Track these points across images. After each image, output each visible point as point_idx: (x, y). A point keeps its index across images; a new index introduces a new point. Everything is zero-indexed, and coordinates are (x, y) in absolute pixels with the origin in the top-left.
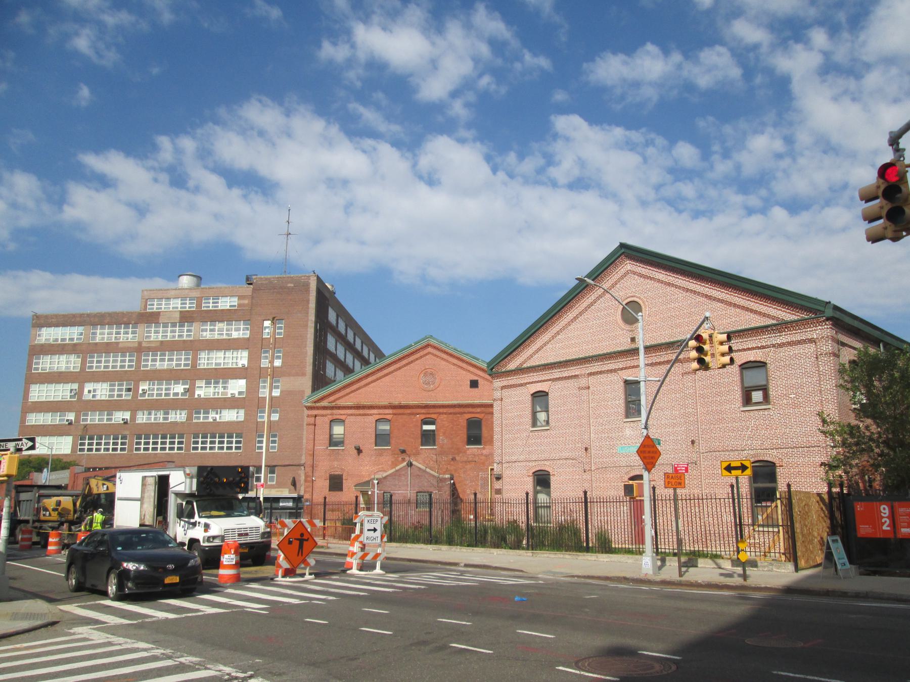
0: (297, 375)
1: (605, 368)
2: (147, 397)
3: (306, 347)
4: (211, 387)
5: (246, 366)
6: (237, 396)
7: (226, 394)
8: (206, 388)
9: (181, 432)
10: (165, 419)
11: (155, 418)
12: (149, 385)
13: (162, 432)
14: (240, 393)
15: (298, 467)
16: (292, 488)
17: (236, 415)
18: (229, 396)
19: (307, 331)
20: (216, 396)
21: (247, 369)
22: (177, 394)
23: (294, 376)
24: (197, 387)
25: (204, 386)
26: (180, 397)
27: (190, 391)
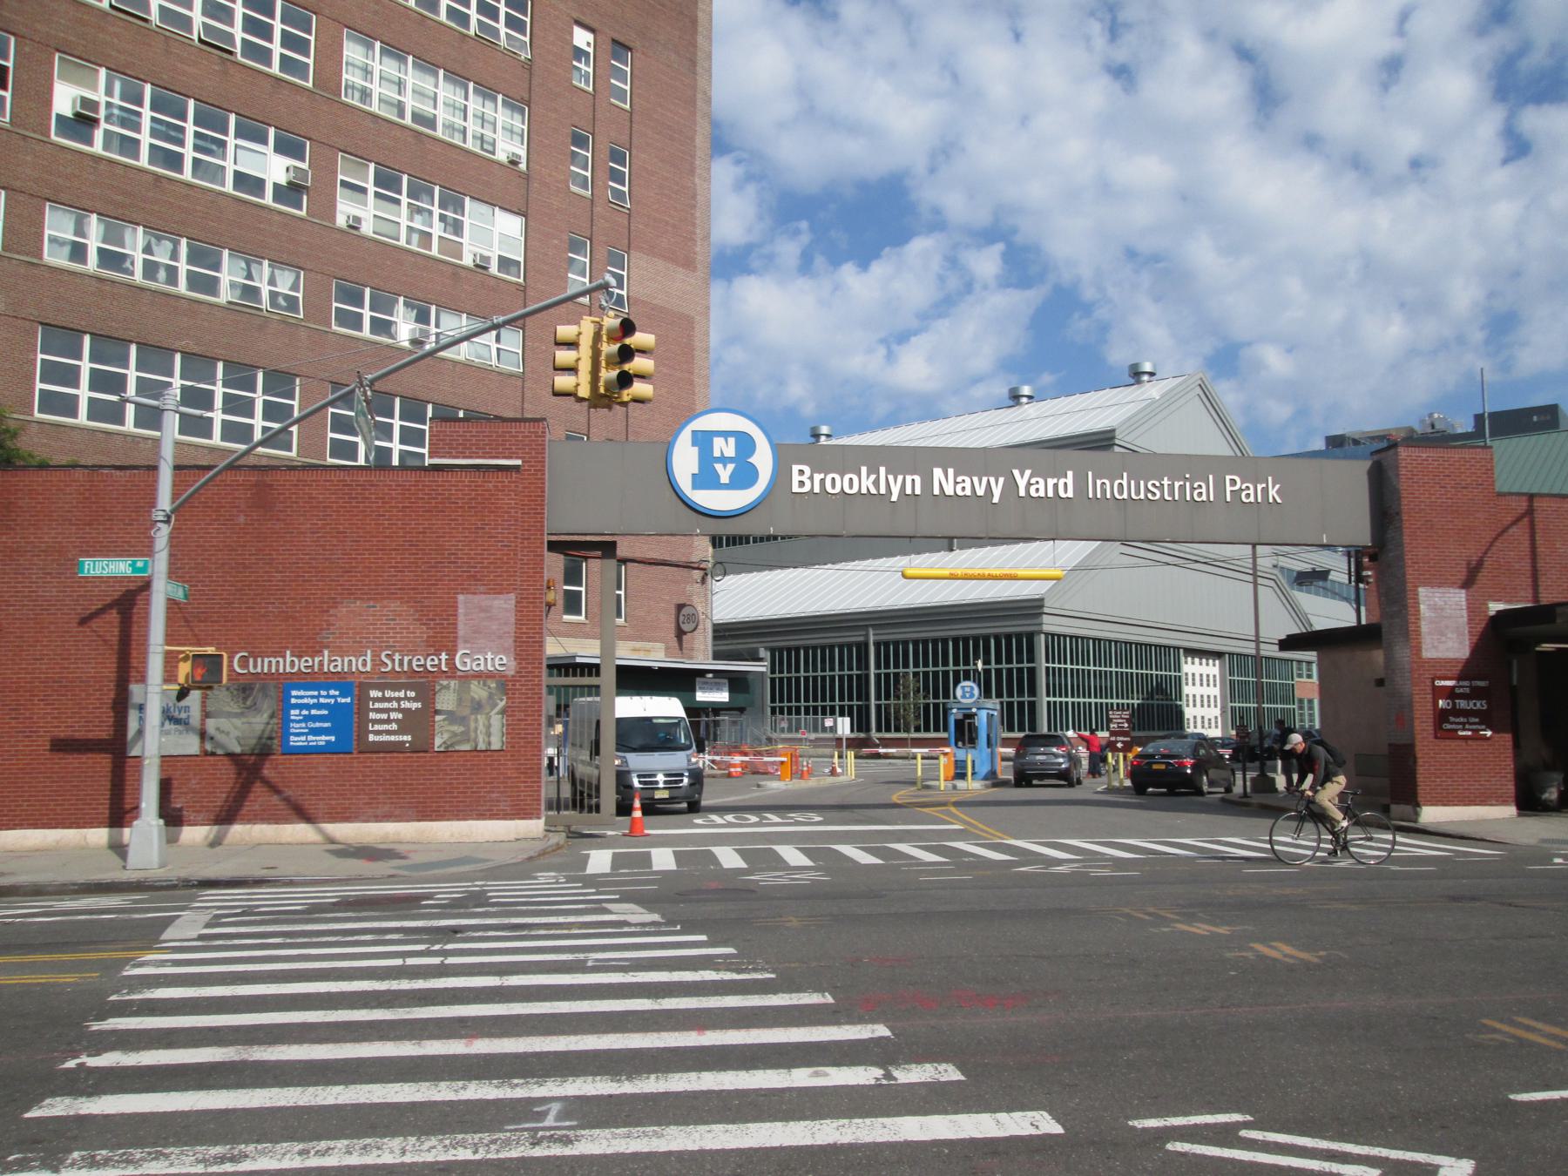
3: (692, 171)
4: (398, 202)
6: (494, 269)
7: (457, 250)
9: (283, 366)
11: (110, 259)
12: (109, 92)
14: (505, 263)
16: (674, 642)
17: (494, 346)
19: (695, 123)
20: (414, 247)
21: (526, 177)
22: (256, 185)
24: (345, 184)
25: (371, 189)
26: (268, 200)
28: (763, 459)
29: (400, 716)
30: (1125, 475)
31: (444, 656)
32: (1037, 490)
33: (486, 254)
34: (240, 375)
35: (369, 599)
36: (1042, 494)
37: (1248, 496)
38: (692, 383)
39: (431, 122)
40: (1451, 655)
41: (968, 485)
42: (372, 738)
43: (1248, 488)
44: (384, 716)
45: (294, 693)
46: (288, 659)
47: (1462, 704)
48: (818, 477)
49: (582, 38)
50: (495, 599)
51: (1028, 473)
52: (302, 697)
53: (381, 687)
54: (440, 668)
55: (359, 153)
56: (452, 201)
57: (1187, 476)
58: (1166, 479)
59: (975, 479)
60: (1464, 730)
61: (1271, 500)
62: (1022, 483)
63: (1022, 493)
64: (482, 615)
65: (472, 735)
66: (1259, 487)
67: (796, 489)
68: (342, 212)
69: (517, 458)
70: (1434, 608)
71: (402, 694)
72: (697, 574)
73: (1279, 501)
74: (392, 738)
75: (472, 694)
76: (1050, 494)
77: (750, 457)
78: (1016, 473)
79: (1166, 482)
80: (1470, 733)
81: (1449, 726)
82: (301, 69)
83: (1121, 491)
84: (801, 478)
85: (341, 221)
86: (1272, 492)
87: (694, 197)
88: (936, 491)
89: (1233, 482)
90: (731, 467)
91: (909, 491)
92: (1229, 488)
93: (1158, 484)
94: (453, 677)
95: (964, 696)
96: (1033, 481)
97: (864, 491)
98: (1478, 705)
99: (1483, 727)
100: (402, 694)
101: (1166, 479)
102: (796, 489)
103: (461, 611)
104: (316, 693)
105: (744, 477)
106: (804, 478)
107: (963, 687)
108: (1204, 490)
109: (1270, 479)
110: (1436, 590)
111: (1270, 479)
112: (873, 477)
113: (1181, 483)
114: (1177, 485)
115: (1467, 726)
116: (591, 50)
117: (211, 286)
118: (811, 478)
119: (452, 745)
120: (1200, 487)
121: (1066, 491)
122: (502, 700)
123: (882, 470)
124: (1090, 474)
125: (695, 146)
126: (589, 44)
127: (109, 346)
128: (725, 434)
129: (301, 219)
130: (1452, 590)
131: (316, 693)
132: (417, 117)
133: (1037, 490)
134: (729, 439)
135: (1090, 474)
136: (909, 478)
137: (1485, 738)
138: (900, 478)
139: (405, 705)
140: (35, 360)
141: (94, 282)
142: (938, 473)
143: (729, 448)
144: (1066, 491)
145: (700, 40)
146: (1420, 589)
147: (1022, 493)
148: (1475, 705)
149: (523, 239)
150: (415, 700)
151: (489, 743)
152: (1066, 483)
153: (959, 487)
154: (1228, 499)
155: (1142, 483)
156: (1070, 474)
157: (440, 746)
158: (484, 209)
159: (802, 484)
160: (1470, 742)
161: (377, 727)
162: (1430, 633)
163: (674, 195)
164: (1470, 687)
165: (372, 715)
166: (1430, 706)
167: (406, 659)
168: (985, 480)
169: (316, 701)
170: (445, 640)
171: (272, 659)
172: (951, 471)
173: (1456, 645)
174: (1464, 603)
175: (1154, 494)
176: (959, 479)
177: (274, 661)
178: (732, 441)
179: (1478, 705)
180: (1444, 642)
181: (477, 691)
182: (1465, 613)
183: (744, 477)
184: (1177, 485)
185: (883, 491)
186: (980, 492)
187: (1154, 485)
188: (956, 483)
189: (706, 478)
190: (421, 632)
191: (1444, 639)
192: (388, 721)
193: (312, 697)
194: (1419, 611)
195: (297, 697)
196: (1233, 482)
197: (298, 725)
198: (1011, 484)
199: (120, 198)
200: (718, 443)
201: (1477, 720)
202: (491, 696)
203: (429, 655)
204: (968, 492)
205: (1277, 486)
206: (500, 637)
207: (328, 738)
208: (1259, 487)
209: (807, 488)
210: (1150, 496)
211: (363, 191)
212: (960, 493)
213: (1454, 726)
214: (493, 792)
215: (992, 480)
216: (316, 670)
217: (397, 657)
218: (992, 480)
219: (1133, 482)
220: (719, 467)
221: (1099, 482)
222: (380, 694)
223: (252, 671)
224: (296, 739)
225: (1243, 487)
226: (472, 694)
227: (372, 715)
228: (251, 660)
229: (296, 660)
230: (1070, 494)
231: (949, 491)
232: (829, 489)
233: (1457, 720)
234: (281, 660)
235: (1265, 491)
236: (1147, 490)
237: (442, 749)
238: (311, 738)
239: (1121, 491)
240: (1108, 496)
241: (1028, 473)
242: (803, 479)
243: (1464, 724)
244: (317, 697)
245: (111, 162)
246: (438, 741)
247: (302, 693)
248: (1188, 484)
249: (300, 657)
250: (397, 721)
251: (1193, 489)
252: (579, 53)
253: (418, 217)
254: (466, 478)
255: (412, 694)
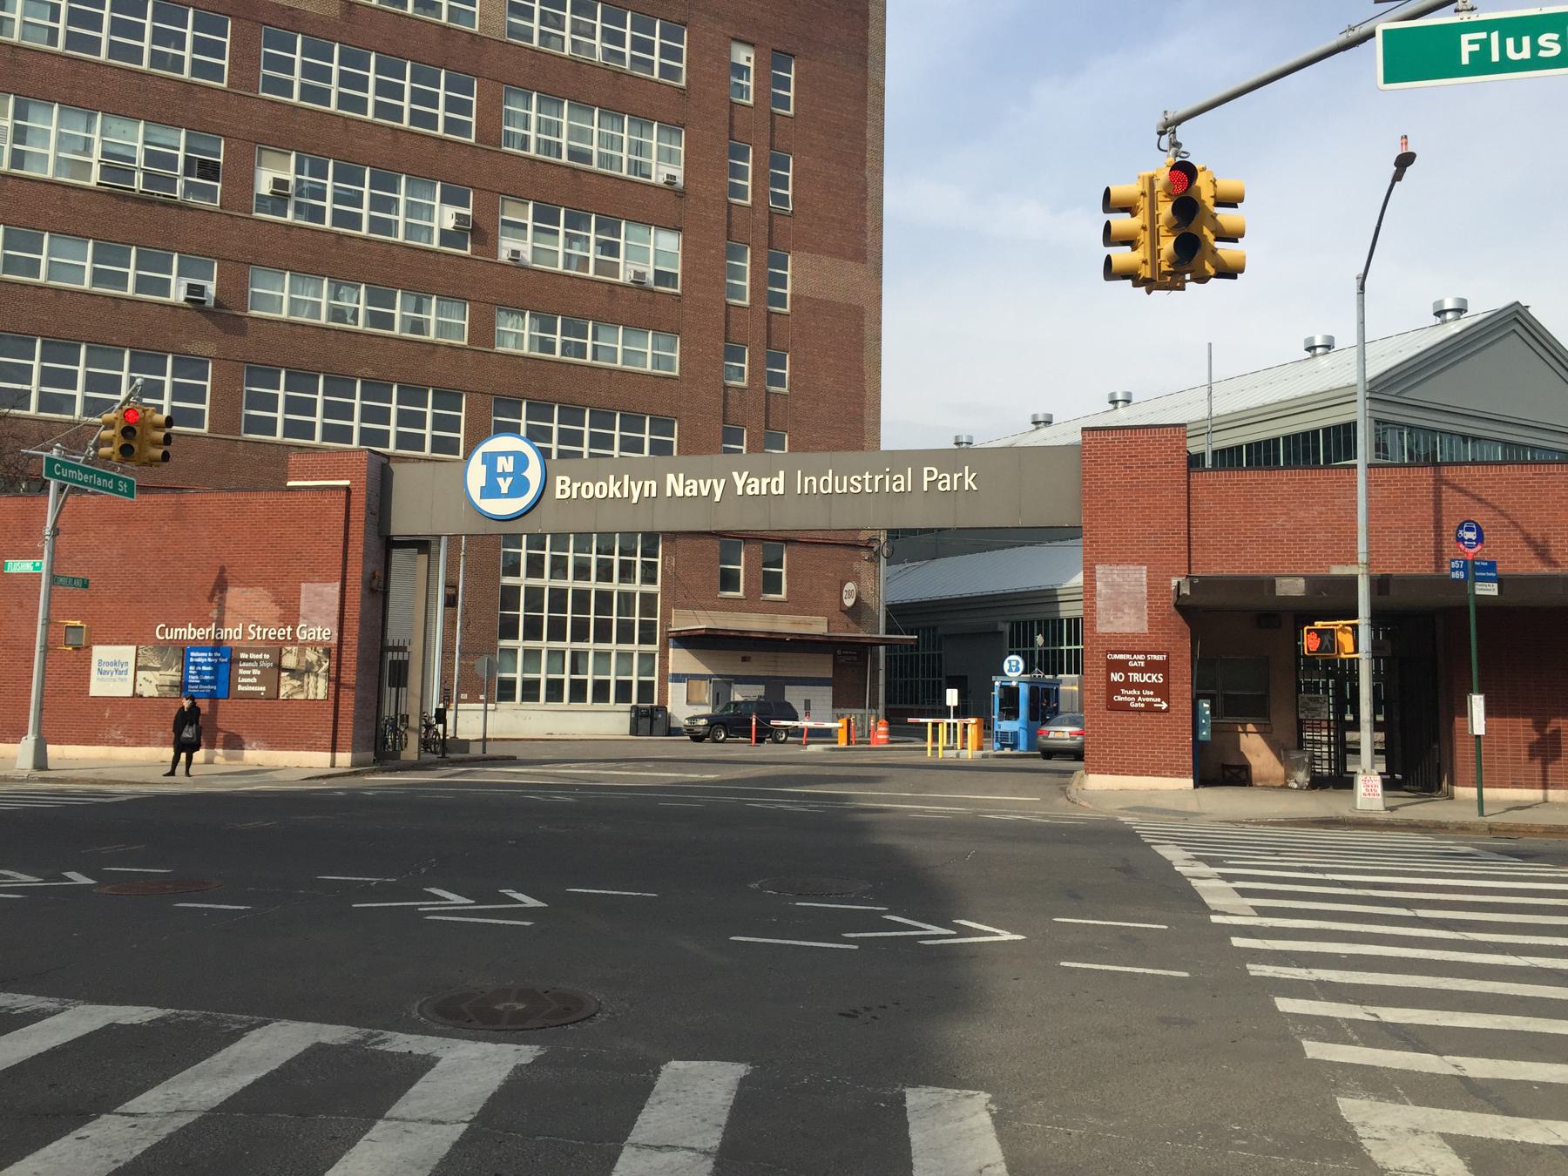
0: (837, 252)
1: (1422, 377)
2: (290, 217)
5: (680, 181)
7: (613, 269)
8: (542, 236)
10: (377, 319)
13: (371, 373)
14: (661, 277)
15: (850, 551)
18: (624, 277)
21: (681, 194)
23: (831, 254)
25: (530, 222)
27: (478, 232)
28: (534, 473)
29: (259, 672)
30: (830, 471)
31: (289, 629)
32: (753, 489)
33: (640, 269)
34: (412, 394)
35: (244, 587)
36: (756, 492)
37: (944, 485)
38: (861, 371)
39: (586, 157)
40: (1127, 630)
41: (695, 487)
42: (240, 688)
43: (944, 478)
44: (248, 672)
45: (193, 654)
46: (190, 630)
47: (1136, 677)
48: (575, 486)
49: (743, 55)
50: (326, 586)
51: (745, 474)
52: (197, 657)
53: (248, 651)
54: (286, 638)
55: (518, 195)
56: (608, 225)
57: (888, 470)
58: (867, 473)
59: (701, 482)
60: (1136, 702)
61: (967, 488)
62: (740, 484)
63: (740, 492)
64: (317, 598)
65: (306, 687)
66: (956, 476)
67: (558, 496)
68: (506, 248)
69: (347, 479)
70: (1107, 584)
71: (260, 656)
72: (865, 554)
73: (975, 488)
74: (253, 688)
75: (307, 657)
76: (764, 492)
77: (524, 471)
78: (735, 475)
79: (867, 476)
80: (1143, 705)
81: (1120, 699)
82: (463, 128)
83: (826, 487)
84: (563, 487)
85: (504, 256)
86: (968, 481)
87: (865, 189)
88: (669, 494)
89: (930, 473)
90: (509, 480)
91: (646, 494)
92: (926, 479)
93: (859, 479)
94: (296, 645)
95: (1010, 670)
96: (750, 481)
97: (611, 496)
98: (1154, 678)
99: (1159, 700)
100: (260, 656)
101: (867, 473)
102: (558, 496)
103: (302, 595)
104: (206, 655)
105: (519, 487)
106: (565, 487)
107: (1010, 662)
108: (902, 482)
109: (967, 468)
110: (1114, 567)
111: (967, 468)
112: (619, 484)
113: (882, 476)
114: (877, 478)
115: (1140, 699)
116: (751, 65)
117: (387, 321)
118: (570, 486)
119: (291, 695)
120: (899, 479)
121: (777, 489)
122: (326, 662)
123: (626, 477)
124: (799, 472)
125: (865, 140)
126: (748, 59)
127: (301, 378)
128: (506, 454)
129: (466, 258)
130: (1131, 567)
131: (206, 655)
132: (574, 154)
133: (753, 489)
134: (509, 457)
135: (799, 472)
136: (647, 483)
137: (1159, 710)
138: (640, 483)
139: (262, 664)
140: (242, 391)
141: (287, 326)
142: (671, 478)
143: (505, 465)
144: (777, 489)
145: (871, 32)
146: (1097, 567)
147: (740, 492)
148: (1150, 678)
149: (680, 253)
150: (268, 661)
151: (316, 694)
152: (777, 482)
153: (688, 489)
154: (925, 489)
155: (845, 478)
156: (782, 473)
157: (284, 696)
158: (639, 231)
159: (563, 491)
160: (1143, 714)
161: (244, 680)
162: (1105, 610)
163: (842, 193)
164: (1145, 660)
165: (241, 672)
166: (1102, 679)
167: (265, 630)
168: (709, 482)
169: (205, 660)
170: (290, 616)
171: (179, 629)
172: (681, 476)
173: (1134, 620)
174: (1145, 579)
175: (856, 488)
176: (688, 482)
177: (181, 630)
178: (511, 459)
179: (1154, 678)
180: (1122, 618)
181: (311, 656)
182: (1145, 590)
183: (519, 487)
184: (877, 478)
185: (626, 495)
186: (705, 493)
187: (855, 479)
188: (685, 486)
189: (491, 491)
190: (277, 611)
191: (1119, 614)
192: (251, 676)
193: (204, 657)
194: (1095, 588)
195: (194, 657)
196: (930, 473)
197: (193, 678)
198: (730, 485)
199: (308, 256)
200: (501, 460)
201: (1152, 693)
202: (319, 660)
203: (280, 627)
204: (695, 493)
205: (974, 474)
206: (328, 615)
207: (212, 687)
208: (956, 476)
209: (566, 495)
210: (852, 489)
211: (524, 226)
212: (688, 494)
213: (1126, 699)
214: (318, 731)
215: (715, 481)
216: (207, 638)
217: (259, 629)
218: (715, 481)
219: (837, 478)
220: (500, 480)
221: (807, 480)
222: (246, 656)
223: (167, 638)
224: (193, 687)
225: (940, 477)
226: (307, 657)
227: (241, 672)
228: (167, 630)
229: (194, 630)
230: (781, 491)
231: (679, 493)
232: (584, 495)
233: (1130, 693)
234: (185, 630)
235: (961, 479)
236: (849, 484)
237: (285, 698)
238: (201, 687)
239: (826, 487)
240: (815, 492)
241: (745, 474)
242: (563, 487)
243: (1136, 697)
244: (207, 657)
245: (301, 228)
246: (283, 692)
247: (197, 654)
248: (887, 477)
249: (197, 628)
250: (256, 676)
251: (891, 482)
252: (740, 70)
253: (576, 244)
254: (309, 495)
255: (267, 656)
